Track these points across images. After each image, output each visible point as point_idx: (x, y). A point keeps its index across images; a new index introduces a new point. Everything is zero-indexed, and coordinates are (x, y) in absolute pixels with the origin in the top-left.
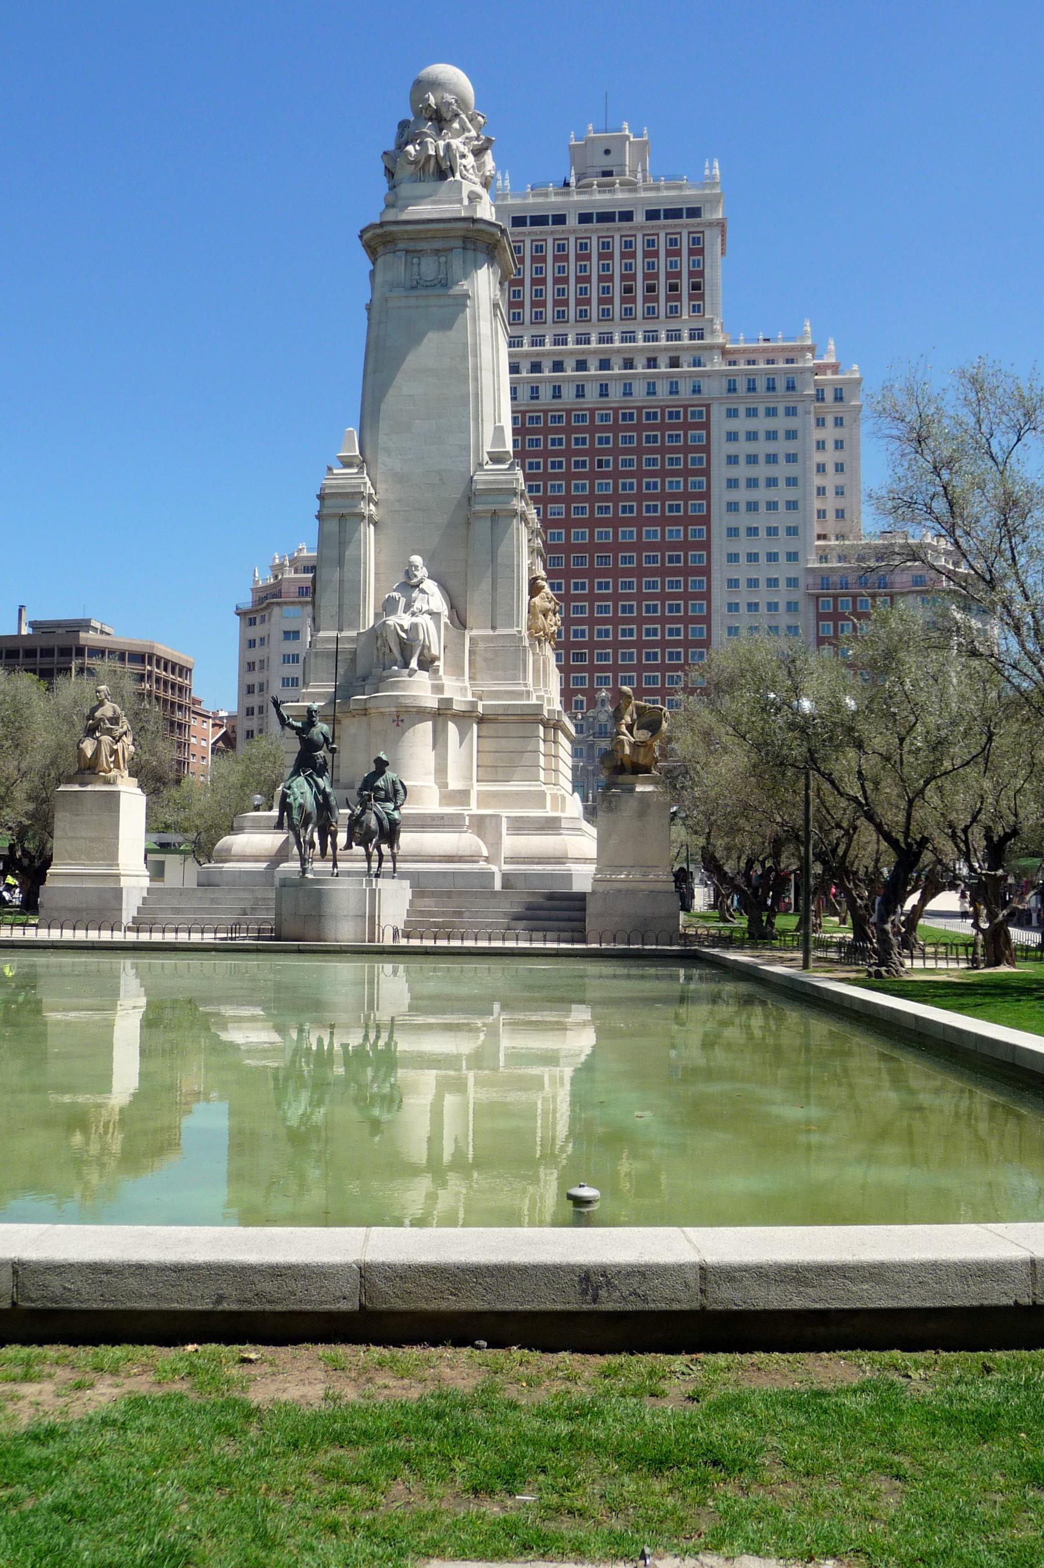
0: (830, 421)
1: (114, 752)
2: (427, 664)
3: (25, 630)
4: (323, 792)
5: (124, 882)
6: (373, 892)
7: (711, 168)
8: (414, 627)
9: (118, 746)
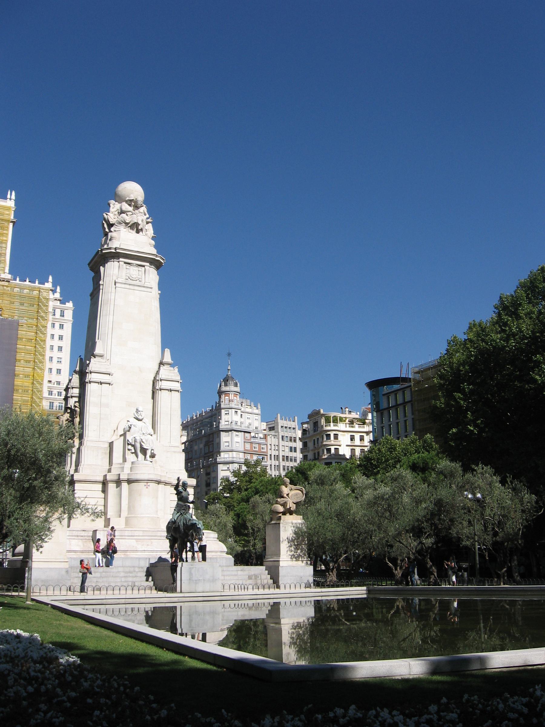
0: (57, 325)
7: (11, 195)
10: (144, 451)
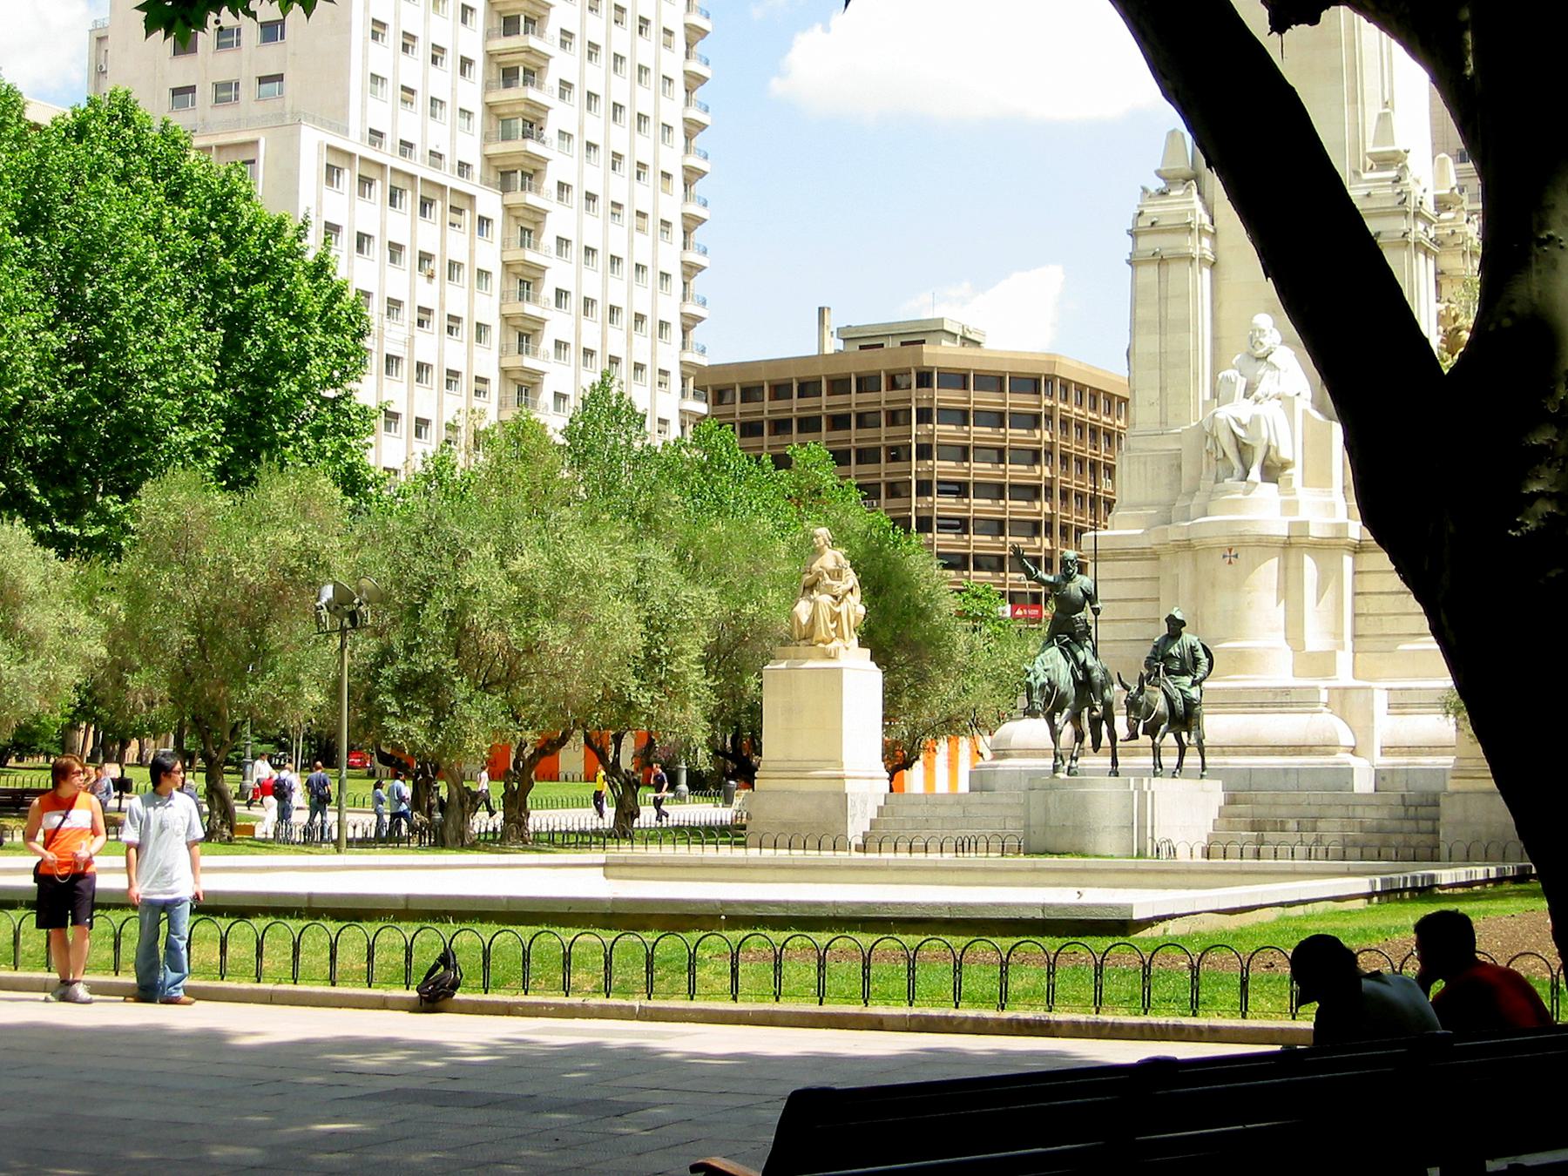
1: (836, 617)
2: (1273, 471)
3: (833, 345)
4: (1083, 667)
5: (849, 787)
6: (1143, 794)
8: (1255, 420)
9: (842, 608)
10: (1243, 449)
